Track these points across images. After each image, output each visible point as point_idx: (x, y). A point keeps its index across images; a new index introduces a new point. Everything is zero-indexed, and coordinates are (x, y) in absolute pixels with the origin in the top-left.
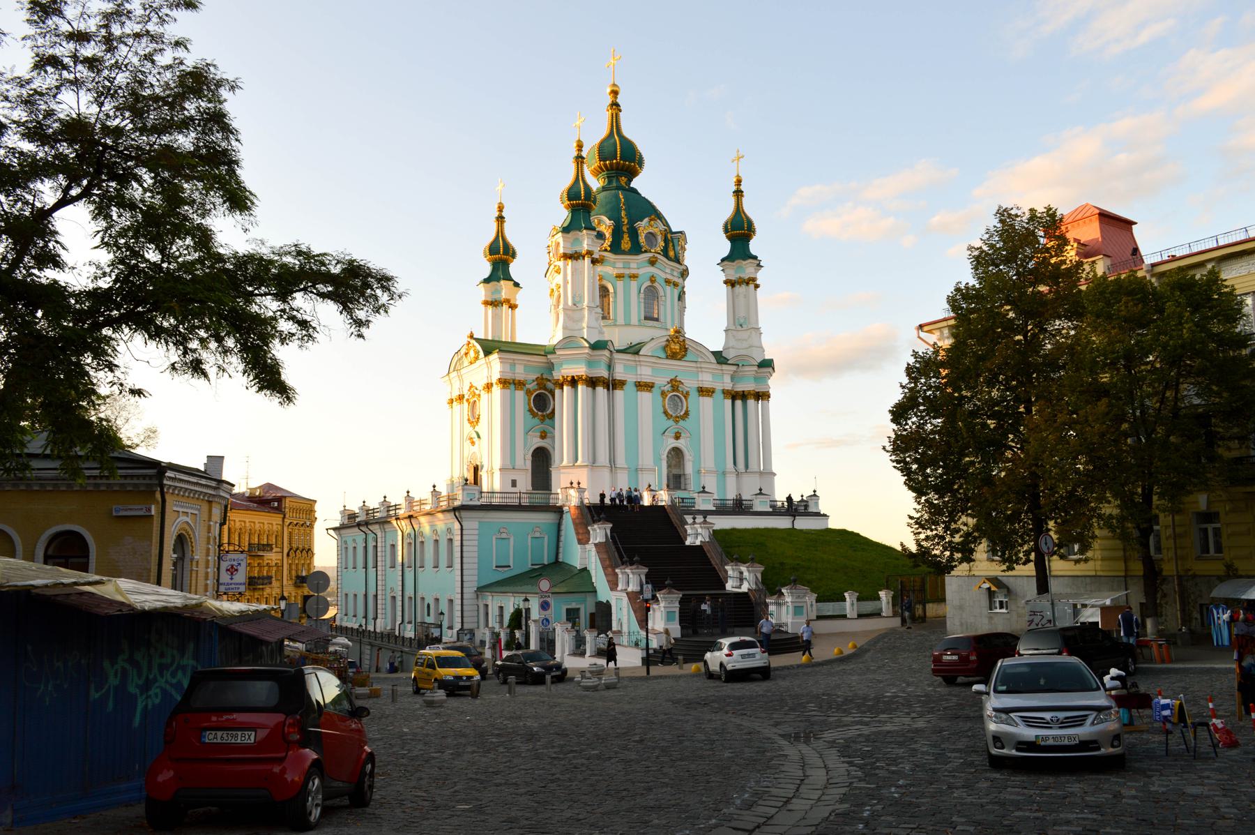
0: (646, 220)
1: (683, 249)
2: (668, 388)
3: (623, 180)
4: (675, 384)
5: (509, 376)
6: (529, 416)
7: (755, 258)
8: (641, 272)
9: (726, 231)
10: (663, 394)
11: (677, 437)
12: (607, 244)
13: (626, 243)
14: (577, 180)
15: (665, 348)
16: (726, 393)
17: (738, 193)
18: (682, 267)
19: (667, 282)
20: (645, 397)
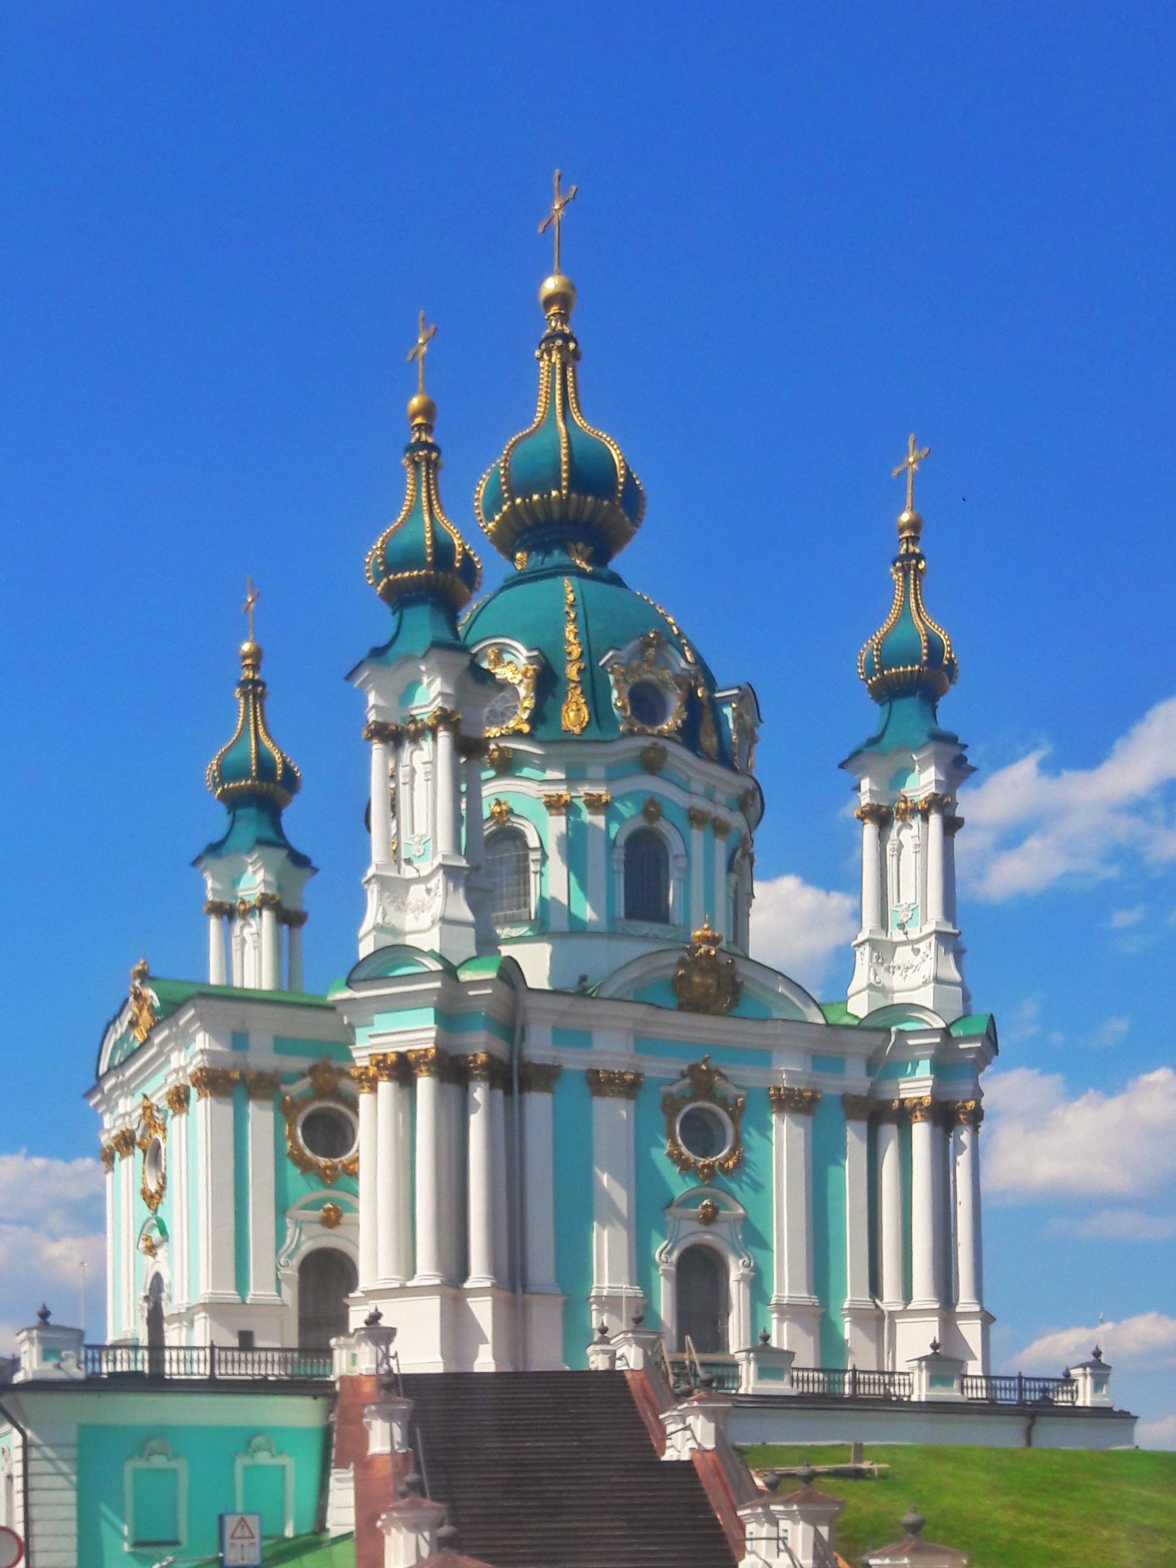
1: (748, 734)
6: (293, 1171)
12: (520, 720)
13: (573, 714)
15: (678, 985)
18: (750, 784)
19: (696, 818)
20: (613, 1115)
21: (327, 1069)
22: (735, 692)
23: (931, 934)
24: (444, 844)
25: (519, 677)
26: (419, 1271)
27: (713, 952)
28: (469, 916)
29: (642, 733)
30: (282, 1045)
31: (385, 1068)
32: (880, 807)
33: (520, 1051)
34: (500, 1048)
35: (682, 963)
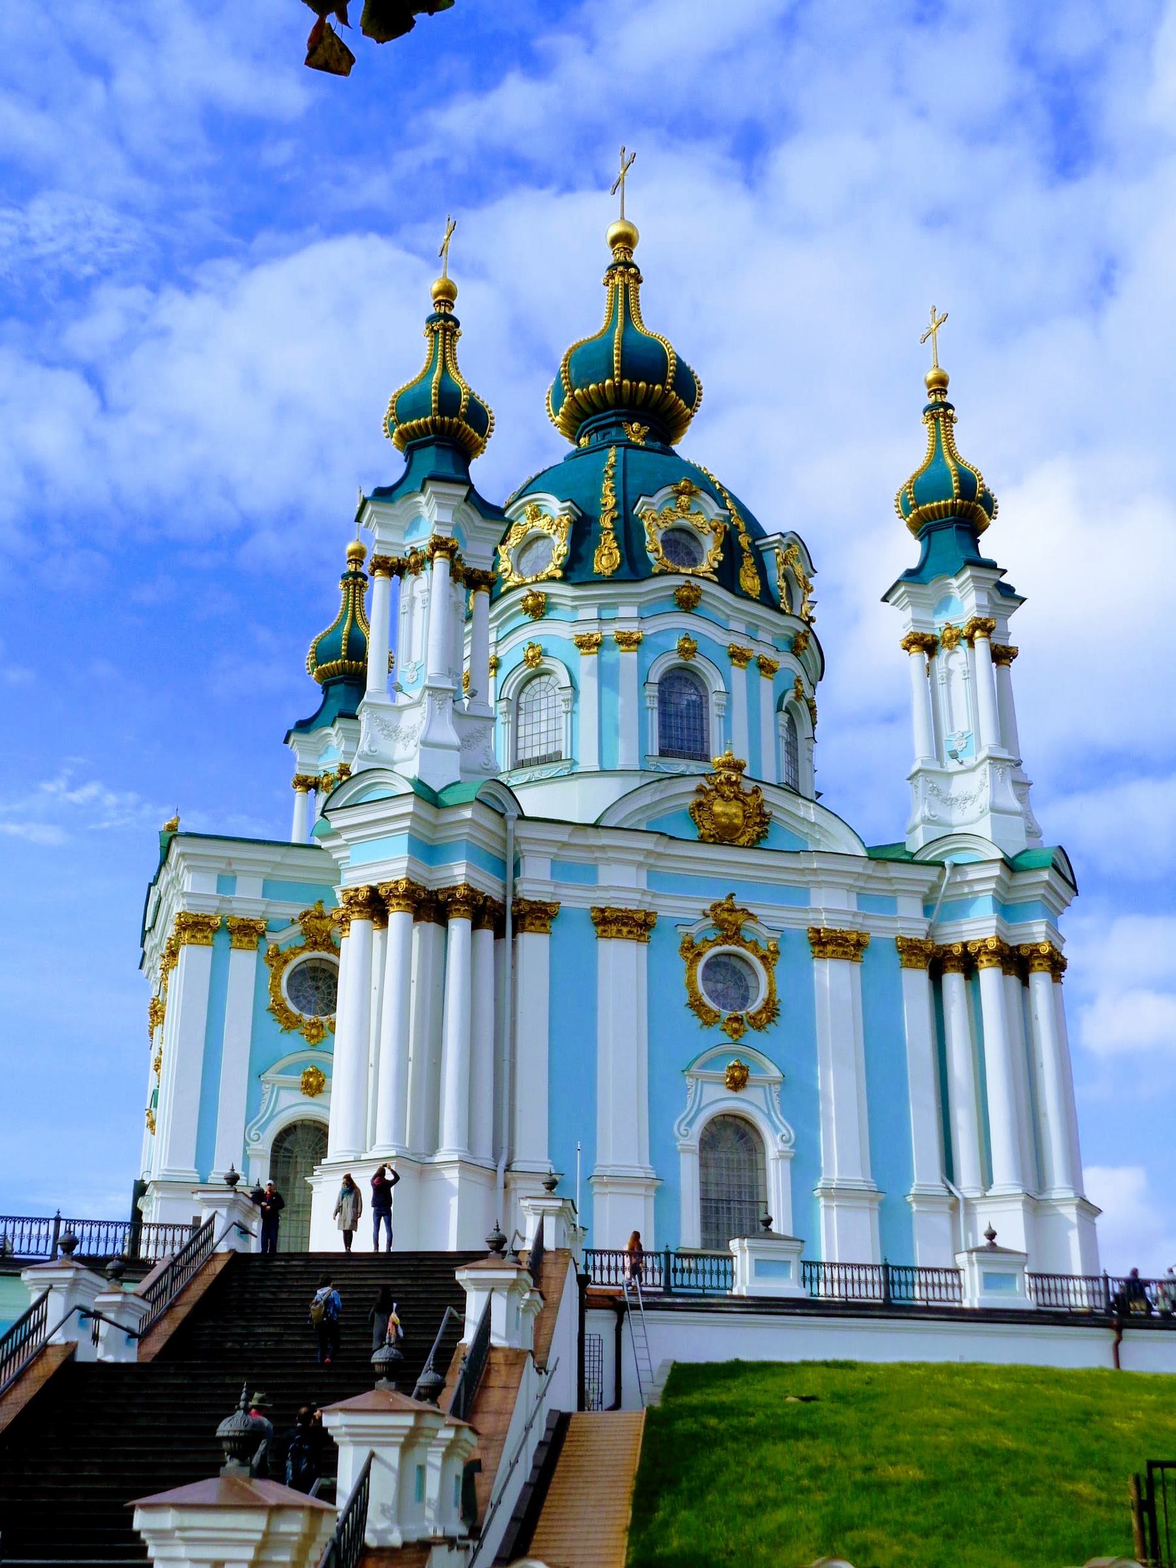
0: (669, 489)
1: (797, 583)
2: (702, 928)
3: (635, 431)
4: (729, 921)
5: (208, 908)
7: (991, 565)
8: (651, 628)
9: (907, 510)
10: (691, 950)
11: (738, 1083)
13: (606, 558)
14: (429, 372)
16: (910, 950)
17: (941, 413)
19: (738, 656)
21: (321, 917)
22: (778, 537)
23: (984, 760)
24: (433, 668)
25: (554, 527)
26: (379, 1141)
27: (734, 778)
28: (455, 739)
29: (678, 573)
30: (268, 888)
31: (356, 903)
32: (923, 636)
33: (515, 887)
34: (490, 886)
35: (700, 790)
